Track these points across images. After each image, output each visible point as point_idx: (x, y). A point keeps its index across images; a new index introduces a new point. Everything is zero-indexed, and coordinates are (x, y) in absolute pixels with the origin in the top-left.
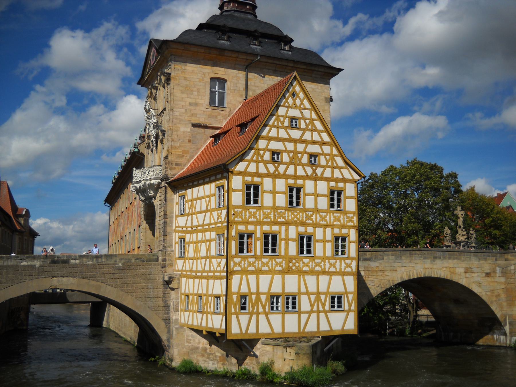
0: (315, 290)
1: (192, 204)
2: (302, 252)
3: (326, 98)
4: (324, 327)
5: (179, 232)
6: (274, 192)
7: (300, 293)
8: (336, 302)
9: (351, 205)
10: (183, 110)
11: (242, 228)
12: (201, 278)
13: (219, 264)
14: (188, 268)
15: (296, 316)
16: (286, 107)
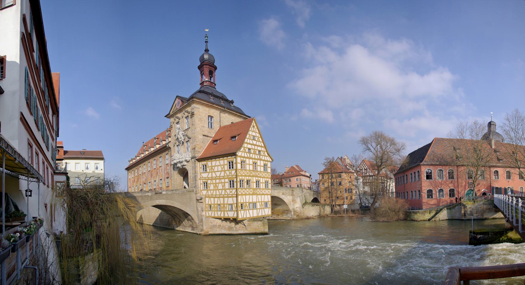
1: (212, 168)
9: (269, 170)
11: (241, 178)
12: (220, 197)
14: (210, 194)
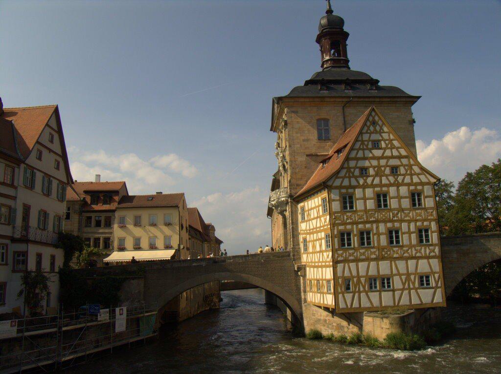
0: (405, 272)
1: (309, 213)
2: (392, 242)
3: (409, 121)
4: (415, 301)
5: (303, 234)
6: (365, 199)
7: (392, 275)
8: (424, 280)
9: (429, 203)
10: (299, 146)
11: (341, 228)
12: (318, 267)
13: (328, 257)
14: (310, 261)
15: (391, 293)
16: (369, 133)
